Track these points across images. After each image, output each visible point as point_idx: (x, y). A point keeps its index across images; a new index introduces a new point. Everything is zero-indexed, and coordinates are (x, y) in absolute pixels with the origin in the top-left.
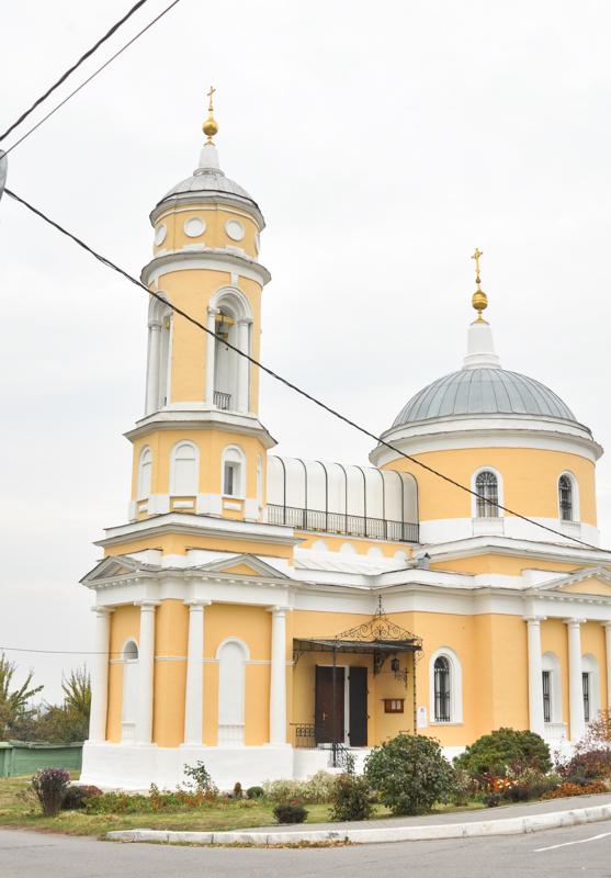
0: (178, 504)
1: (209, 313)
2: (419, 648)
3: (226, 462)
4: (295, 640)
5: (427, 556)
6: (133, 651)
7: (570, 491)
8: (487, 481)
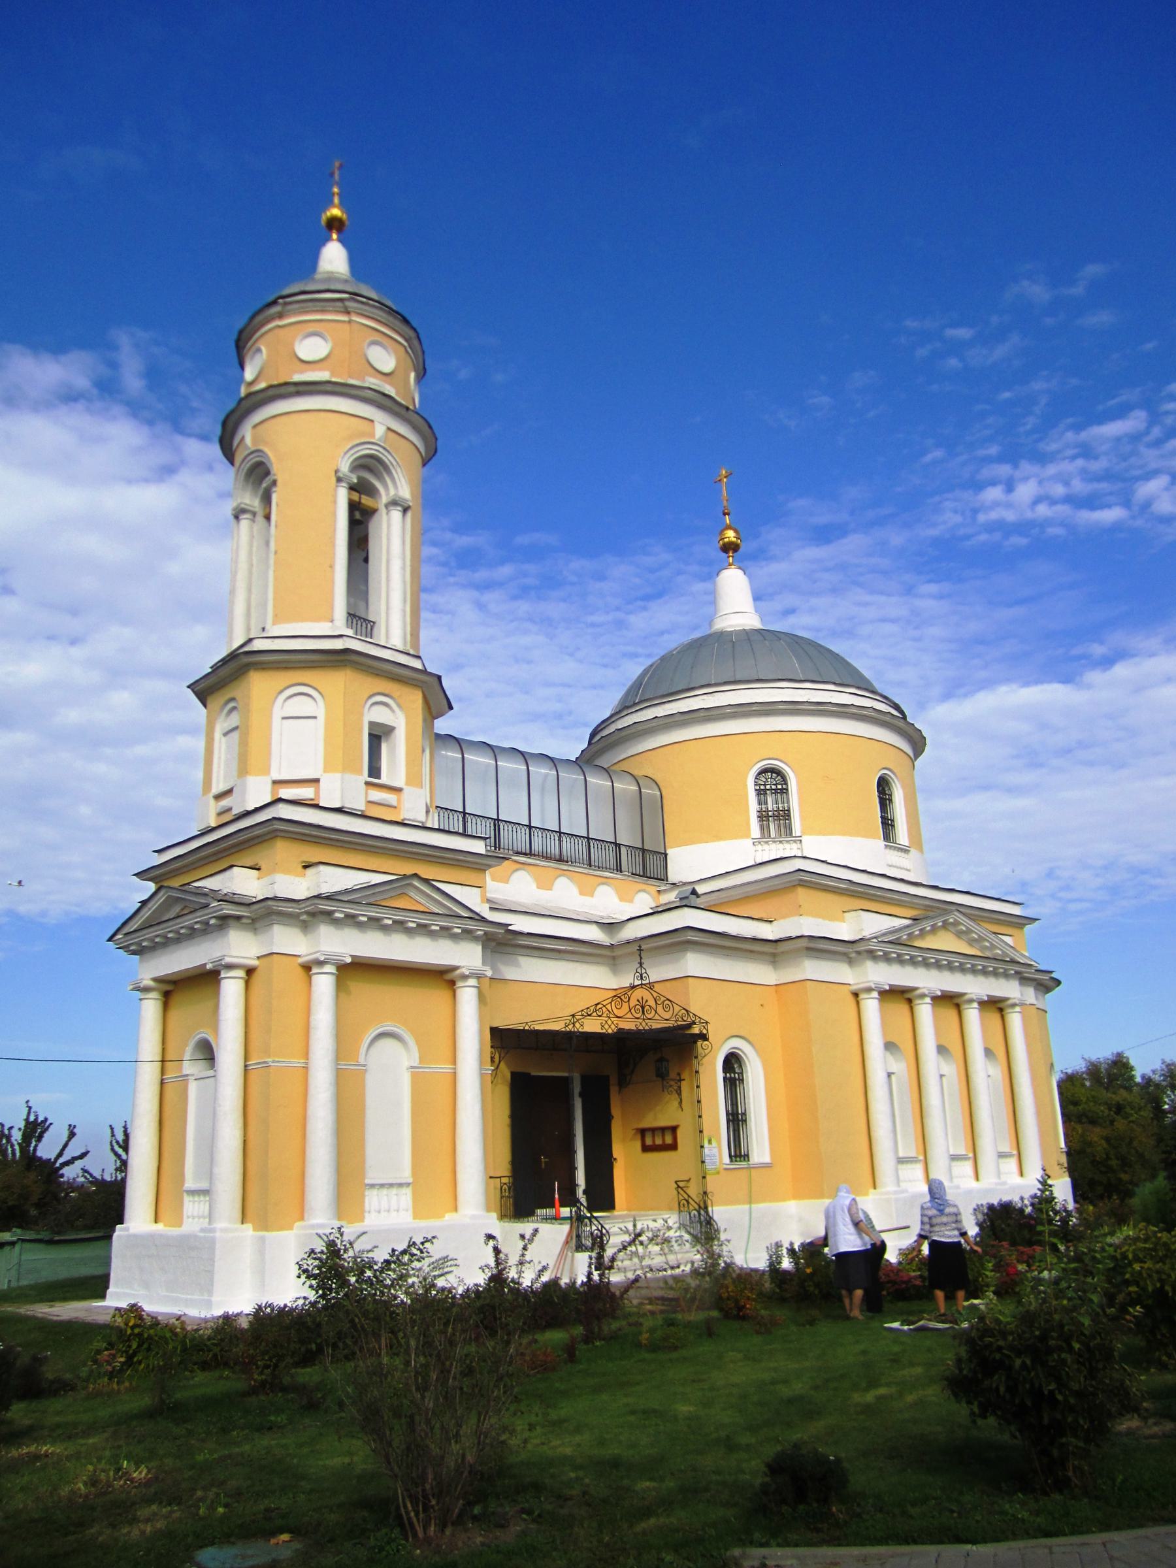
0: (286, 793)
1: (339, 480)
2: (703, 1037)
3: (372, 724)
4: (494, 1030)
5: (694, 892)
6: (207, 1053)
7: (891, 801)
8: (773, 781)
